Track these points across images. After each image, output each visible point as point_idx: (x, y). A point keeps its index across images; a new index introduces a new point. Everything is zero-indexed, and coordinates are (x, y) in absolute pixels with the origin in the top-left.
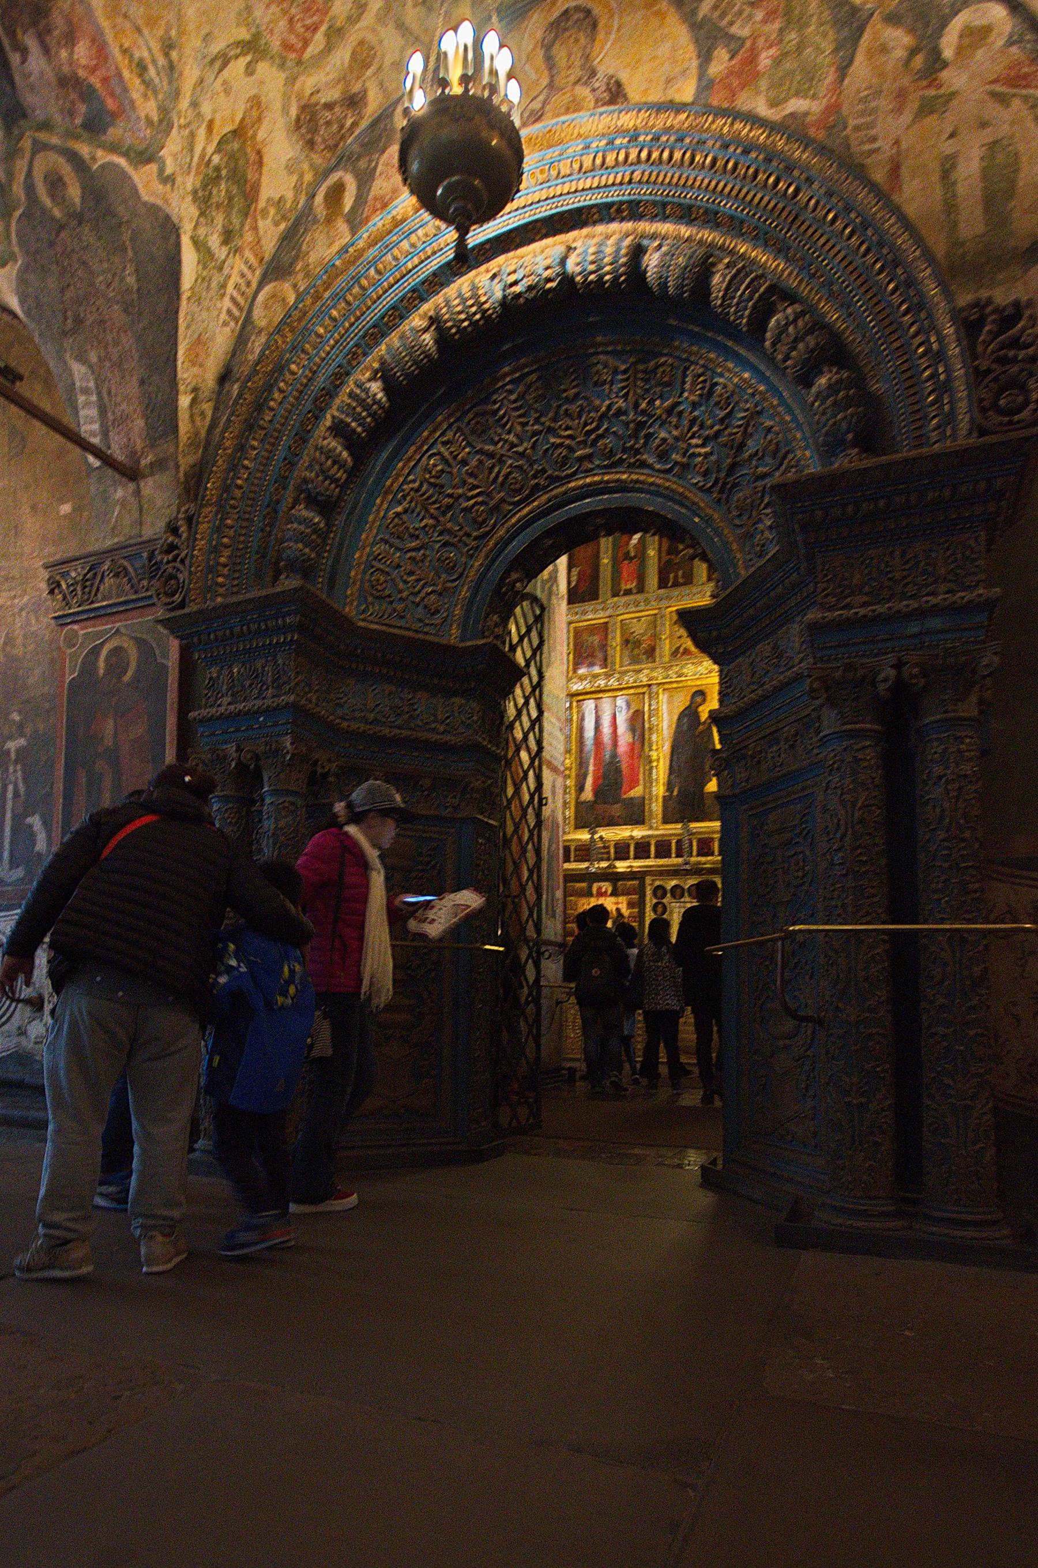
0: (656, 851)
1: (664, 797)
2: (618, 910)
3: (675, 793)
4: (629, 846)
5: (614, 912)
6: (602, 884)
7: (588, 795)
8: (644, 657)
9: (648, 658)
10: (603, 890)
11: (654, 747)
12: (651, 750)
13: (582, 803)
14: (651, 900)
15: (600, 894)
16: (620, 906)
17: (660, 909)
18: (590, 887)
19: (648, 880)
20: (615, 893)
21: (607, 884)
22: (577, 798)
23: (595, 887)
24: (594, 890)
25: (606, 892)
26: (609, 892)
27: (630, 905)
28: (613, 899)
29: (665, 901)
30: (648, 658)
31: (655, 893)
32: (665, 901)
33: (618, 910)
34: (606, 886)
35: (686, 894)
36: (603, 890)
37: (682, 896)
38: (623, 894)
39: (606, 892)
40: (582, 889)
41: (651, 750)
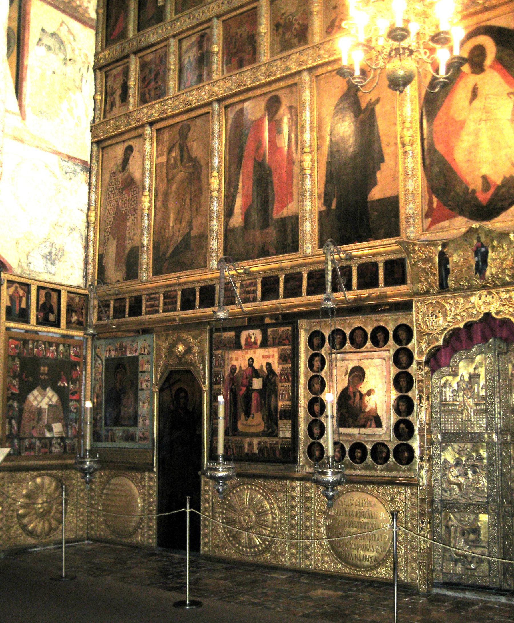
1: (320, 213)
2: (269, 365)
3: (334, 207)
4: (277, 280)
5: (265, 369)
6: (251, 332)
7: (237, 220)
8: (296, 40)
9: (299, 41)
10: (253, 340)
11: (307, 150)
12: (303, 153)
14: (306, 351)
15: (250, 345)
16: (270, 361)
17: (317, 363)
18: (238, 337)
19: (303, 323)
20: (264, 344)
22: (226, 224)
24: (243, 342)
25: (255, 343)
26: (259, 342)
27: (283, 359)
28: (261, 352)
29: (323, 352)
30: (299, 41)
31: (310, 342)
32: (323, 352)
33: (269, 365)
34: (256, 335)
35: (348, 344)
37: (343, 344)
38: (274, 345)
39: (255, 343)
40: (230, 340)
41: (303, 153)
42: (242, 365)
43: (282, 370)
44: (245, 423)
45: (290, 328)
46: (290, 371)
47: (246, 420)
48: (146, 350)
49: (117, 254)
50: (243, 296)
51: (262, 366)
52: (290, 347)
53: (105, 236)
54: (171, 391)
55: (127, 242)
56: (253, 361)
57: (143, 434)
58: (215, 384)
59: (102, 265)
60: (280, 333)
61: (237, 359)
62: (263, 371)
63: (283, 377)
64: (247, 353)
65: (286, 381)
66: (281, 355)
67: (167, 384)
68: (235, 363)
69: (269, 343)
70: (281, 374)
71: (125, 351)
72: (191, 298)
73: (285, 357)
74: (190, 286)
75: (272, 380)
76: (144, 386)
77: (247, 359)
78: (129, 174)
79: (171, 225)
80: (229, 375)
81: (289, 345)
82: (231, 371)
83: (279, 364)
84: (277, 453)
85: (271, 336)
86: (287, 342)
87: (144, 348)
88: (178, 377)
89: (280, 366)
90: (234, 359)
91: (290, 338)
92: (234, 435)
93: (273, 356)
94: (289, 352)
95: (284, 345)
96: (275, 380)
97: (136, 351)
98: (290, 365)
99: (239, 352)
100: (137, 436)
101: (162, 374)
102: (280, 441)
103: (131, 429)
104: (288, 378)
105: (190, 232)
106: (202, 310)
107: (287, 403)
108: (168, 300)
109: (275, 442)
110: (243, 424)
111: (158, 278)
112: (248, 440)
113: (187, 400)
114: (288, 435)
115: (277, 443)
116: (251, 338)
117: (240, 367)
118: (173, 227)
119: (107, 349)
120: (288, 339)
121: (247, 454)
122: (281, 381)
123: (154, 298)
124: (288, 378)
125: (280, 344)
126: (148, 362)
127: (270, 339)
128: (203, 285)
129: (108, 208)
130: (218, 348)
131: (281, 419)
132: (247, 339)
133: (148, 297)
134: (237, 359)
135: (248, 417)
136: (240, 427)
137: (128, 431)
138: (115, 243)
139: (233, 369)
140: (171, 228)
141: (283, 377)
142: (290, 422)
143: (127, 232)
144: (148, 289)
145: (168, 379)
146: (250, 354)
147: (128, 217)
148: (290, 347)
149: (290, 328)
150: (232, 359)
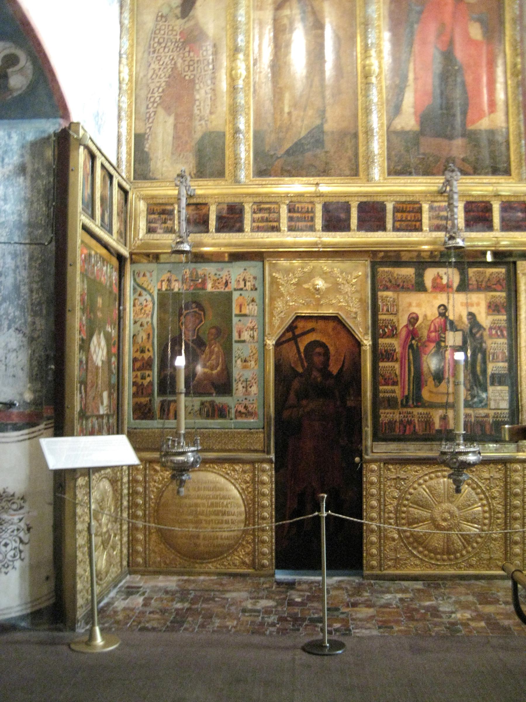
0: (503, 220)
5: (465, 319)
6: (442, 271)
10: (445, 281)
13: (396, 133)
16: (473, 310)
18: (420, 275)
21: (450, 270)
23: (430, 274)
26: (456, 284)
28: (460, 297)
36: (445, 281)
38: (479, 289)
40: (405, 279)
42: (429, 314)
43: (493, 322)
44: (434, 390)
45: (503, 270)
46: (504, 324)
47: (436, 386)
48: (248, 284)
49: (176, 137)
50: (436, 222)
51: (461, 317)
52: (504, 294)
53: (147, 108)
54: (296, 344)
55: (197, 123)
56: (445, 308)
57: (246, 407)
58: (382, 337)
59: (143, 151)
60: (488, 275)
61: (419, 305)
62: (463, 323)
63: (494, 332)
64: (435, 298)
65: (498, 337)
66: (490, 303)
67: (290, 335)
68: (414, 309)
69: (470, 287)
70: (491, 328)
71: (204, 282)
72: (343, 216)
73: (496, 306)
74: (343, 200)
75: (478, 335)
76: (246, 336)
77: (437, 305)
78: (197, 24)
79: (286, 110)
80: (406, 326)
81: (501, 291)
82: (409, 321)
83: (488, 314)
84: (488, 427)
85: (474, 279)
86: (499, 287)
87: (244, 280)
88: (310, 325)
89: (491, 318)
90: (414, 304)
91: (504, 283)
92: (417, 407)
93: (478, 304)
94: (503, 300)
95: (495, 290)
96: (482, 335)
97: (226, 284)
98: (505, 317)
99: (422, 296)
100: (233, 411)
101: (282, 320)
102: (492, 413)
103: (220, 400)
104: (502, 331)
105: (322, 124)
106: (362, 234)
107: (501, 364)
108: (295, 215)
109: (483, 415)
110: (431, 392)
111: (259, 181)
112: (441, 412)
113: (328, 359)
114: (505, 405)
115: (487, 416)
116: (441, 278)
117: (425, 316)
118: (289, 113)
119: (165, 276)
120: (501, 285)
121: (439, 431)
122: (491, 336)
123: (269, 209)
124: (502, 331)
125: (489, 288)
126: (253, 301)
127: (473, 282)
128: (364, 199)
129: (153, 66)
130: (387, 289)
131: (492, 384)
132: (434, 280)
133: (255, 207)
134: (419, 305)
135: (440, 382)
136: (425, 394)
137: (212, 403)
138: (171, 120)
139: (413, 319)
140: (286, 115)
141: (494, 332)
142: (506, 388)
143: (195, 108)
144: (258, 195)
145: (291, 328)
146: (441, 299)
147: (197, 87)
148: (504, 294)
149: (503, 270)
150: (410, 305)
